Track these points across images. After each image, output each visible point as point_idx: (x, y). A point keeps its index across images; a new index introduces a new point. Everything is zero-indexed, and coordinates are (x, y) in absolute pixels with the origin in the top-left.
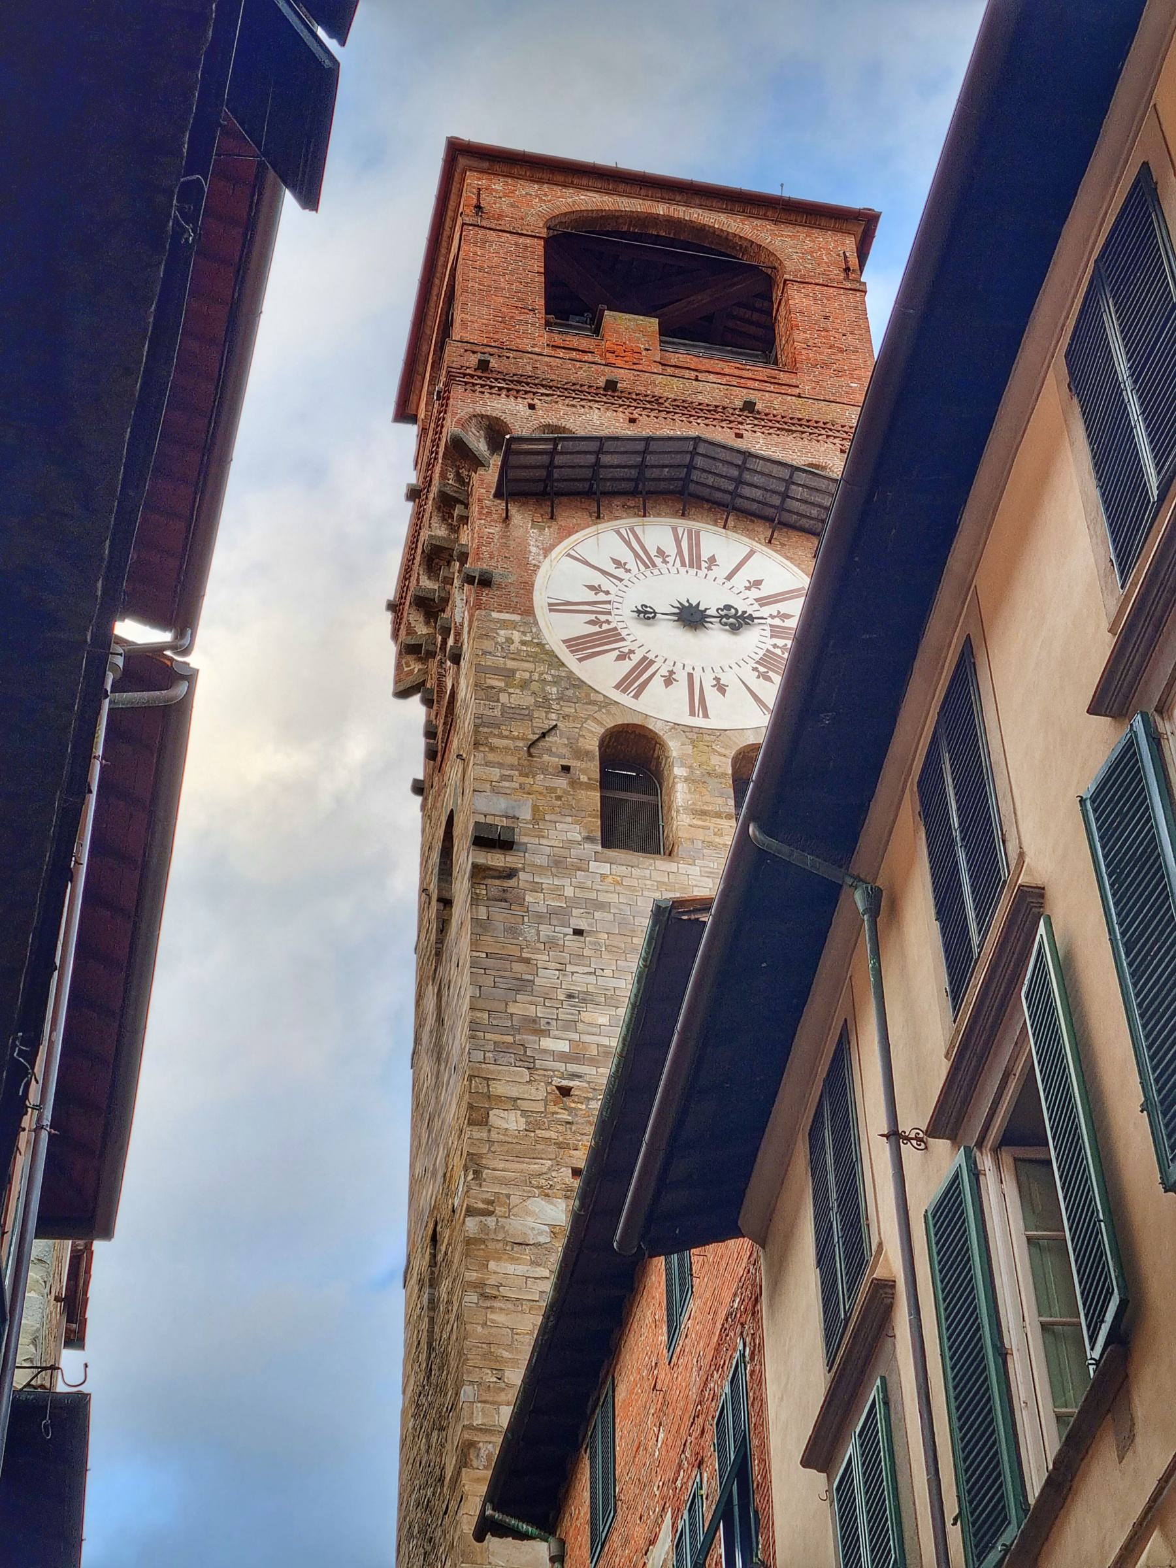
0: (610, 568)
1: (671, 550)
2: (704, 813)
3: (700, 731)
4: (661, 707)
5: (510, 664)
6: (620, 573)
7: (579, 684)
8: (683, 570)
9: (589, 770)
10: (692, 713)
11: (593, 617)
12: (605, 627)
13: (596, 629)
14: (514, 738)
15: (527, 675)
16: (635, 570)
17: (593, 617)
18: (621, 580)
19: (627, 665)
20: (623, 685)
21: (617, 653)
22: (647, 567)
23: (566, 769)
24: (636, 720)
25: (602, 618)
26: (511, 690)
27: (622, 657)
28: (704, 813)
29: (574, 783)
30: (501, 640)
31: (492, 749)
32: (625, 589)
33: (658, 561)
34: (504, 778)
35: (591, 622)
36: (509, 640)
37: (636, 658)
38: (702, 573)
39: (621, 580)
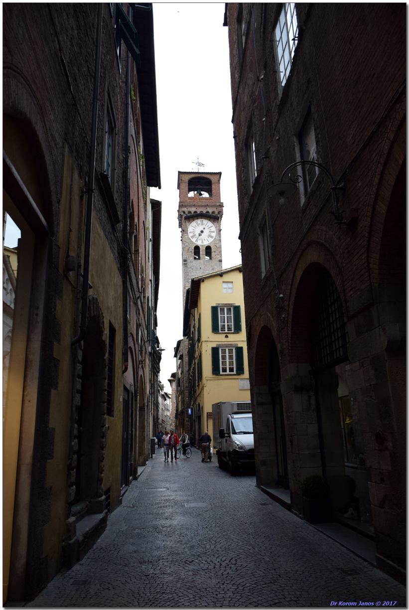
4: (199, 243)
9: (193, 251)
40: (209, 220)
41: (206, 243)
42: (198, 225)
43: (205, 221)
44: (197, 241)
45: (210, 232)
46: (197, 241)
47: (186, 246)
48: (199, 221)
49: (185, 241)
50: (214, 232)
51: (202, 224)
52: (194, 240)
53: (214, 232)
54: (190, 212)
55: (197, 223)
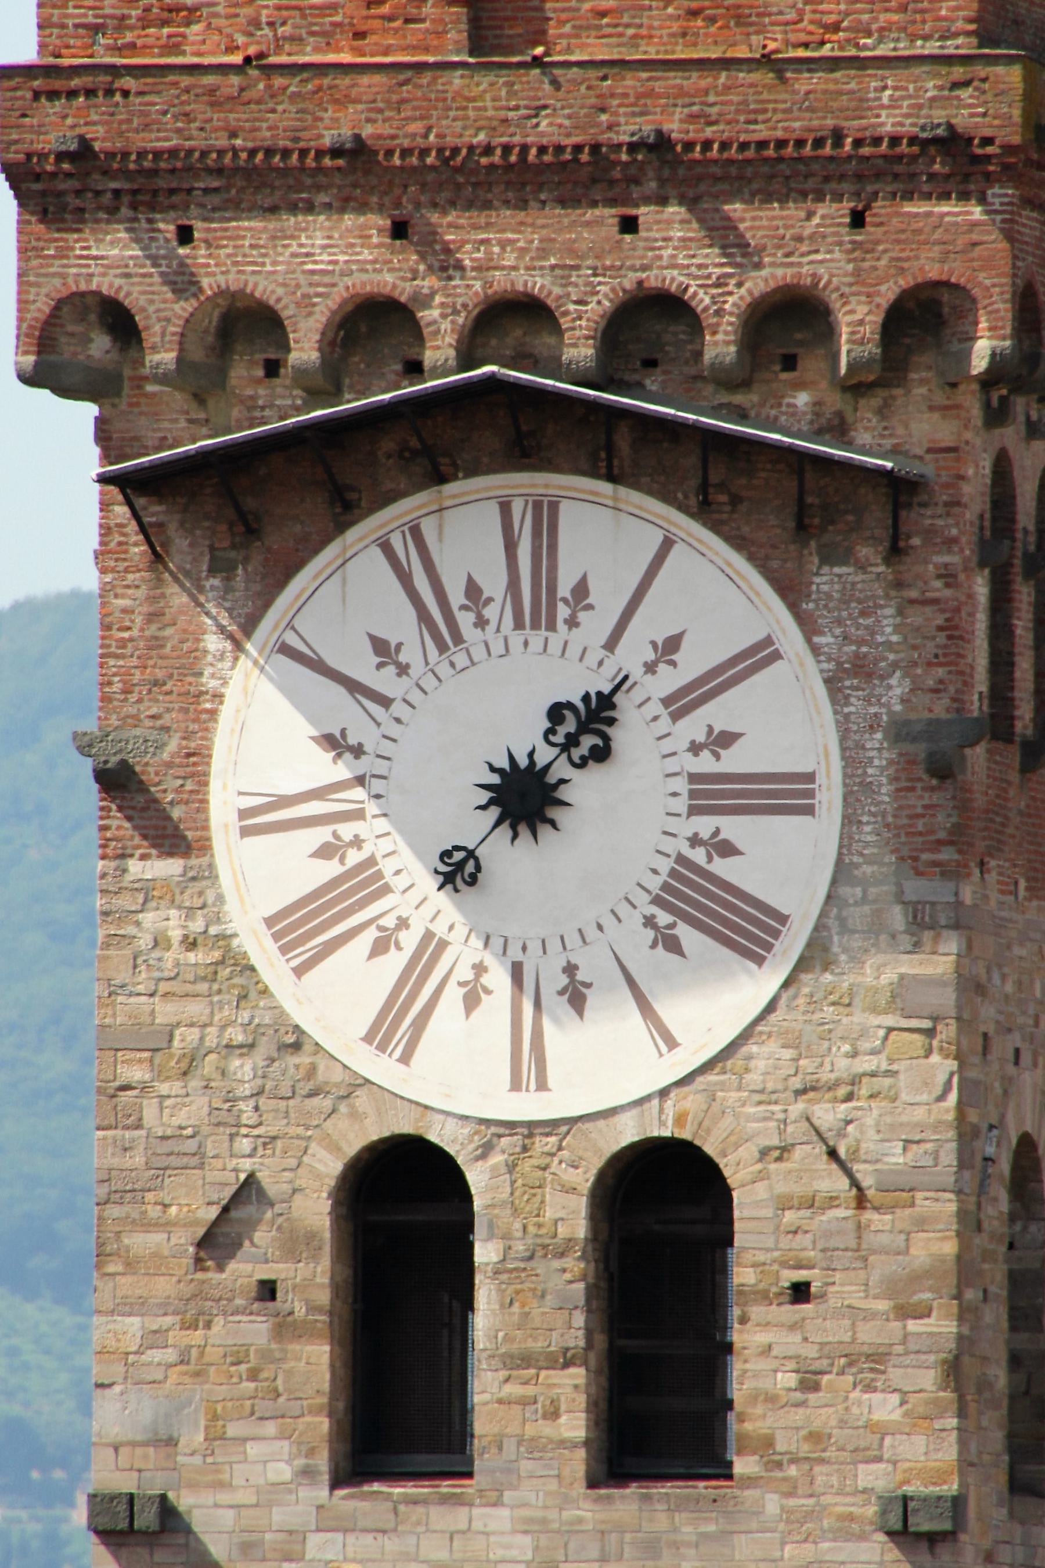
0: (363, 667)
1: (494, 585)
2: (526, 1360)
3: (532, 1128)
4: (454, 1080)
5: (165, 1012)
6: (385, 681)
7: (297, 1042)
8: (516, 640)
9: (313, 1279)
10: (516, 1085)
11: (322, 834)
12: (354, 857)
13: (331, 869)
14: (166, 1226)
15: (193, 1035)
16: (417, 668)
17: (322, 834)
18: (385, 702)
19: (395, 962)
20: (379, 1036)
21: (371, 934)
22: (442, 648)
23: (268, 1290)
24: (406, 1127)
25: (347, 830)
26: (164, 1088)
27: (380, 948)
28: (526, 1360)
29: (285, 1329)
30: (144, 941)
31: (131, 1266)
32: (394, 730)
33: (465, 620)
34: (154, 1339)
35: (325, 852)
36: (160, 942)
37: (410, 940)
38: (556, 641)
39: (385, 702)
40: (704, 510)
41: (613, 1074)
42: (443, 635)
43: (606, 531)
44: (398, 1024)
45: (710, 795)
46: (398, 1024)
47: (177, 1154)
48: (467, 527)
49: (154, 1044)
50: (784, 795)
51: (543, 604)
52: (333, 1002)
53: (784, 795)
54: (247, 325)
55: (412, 567)
